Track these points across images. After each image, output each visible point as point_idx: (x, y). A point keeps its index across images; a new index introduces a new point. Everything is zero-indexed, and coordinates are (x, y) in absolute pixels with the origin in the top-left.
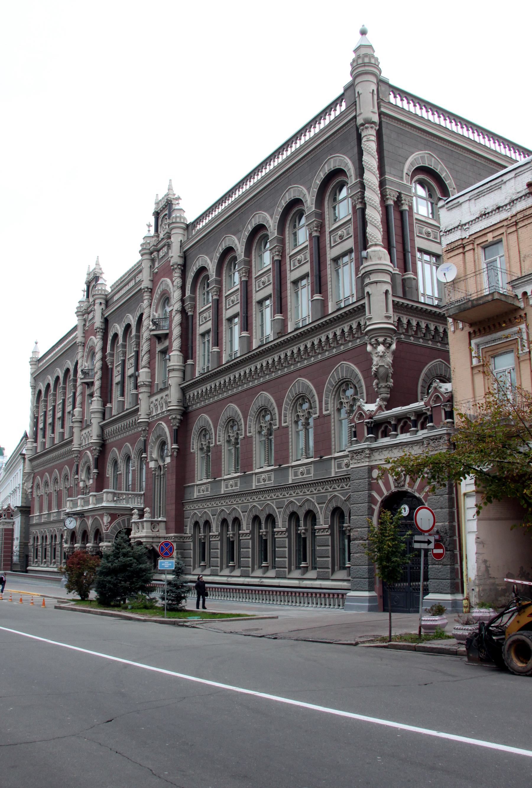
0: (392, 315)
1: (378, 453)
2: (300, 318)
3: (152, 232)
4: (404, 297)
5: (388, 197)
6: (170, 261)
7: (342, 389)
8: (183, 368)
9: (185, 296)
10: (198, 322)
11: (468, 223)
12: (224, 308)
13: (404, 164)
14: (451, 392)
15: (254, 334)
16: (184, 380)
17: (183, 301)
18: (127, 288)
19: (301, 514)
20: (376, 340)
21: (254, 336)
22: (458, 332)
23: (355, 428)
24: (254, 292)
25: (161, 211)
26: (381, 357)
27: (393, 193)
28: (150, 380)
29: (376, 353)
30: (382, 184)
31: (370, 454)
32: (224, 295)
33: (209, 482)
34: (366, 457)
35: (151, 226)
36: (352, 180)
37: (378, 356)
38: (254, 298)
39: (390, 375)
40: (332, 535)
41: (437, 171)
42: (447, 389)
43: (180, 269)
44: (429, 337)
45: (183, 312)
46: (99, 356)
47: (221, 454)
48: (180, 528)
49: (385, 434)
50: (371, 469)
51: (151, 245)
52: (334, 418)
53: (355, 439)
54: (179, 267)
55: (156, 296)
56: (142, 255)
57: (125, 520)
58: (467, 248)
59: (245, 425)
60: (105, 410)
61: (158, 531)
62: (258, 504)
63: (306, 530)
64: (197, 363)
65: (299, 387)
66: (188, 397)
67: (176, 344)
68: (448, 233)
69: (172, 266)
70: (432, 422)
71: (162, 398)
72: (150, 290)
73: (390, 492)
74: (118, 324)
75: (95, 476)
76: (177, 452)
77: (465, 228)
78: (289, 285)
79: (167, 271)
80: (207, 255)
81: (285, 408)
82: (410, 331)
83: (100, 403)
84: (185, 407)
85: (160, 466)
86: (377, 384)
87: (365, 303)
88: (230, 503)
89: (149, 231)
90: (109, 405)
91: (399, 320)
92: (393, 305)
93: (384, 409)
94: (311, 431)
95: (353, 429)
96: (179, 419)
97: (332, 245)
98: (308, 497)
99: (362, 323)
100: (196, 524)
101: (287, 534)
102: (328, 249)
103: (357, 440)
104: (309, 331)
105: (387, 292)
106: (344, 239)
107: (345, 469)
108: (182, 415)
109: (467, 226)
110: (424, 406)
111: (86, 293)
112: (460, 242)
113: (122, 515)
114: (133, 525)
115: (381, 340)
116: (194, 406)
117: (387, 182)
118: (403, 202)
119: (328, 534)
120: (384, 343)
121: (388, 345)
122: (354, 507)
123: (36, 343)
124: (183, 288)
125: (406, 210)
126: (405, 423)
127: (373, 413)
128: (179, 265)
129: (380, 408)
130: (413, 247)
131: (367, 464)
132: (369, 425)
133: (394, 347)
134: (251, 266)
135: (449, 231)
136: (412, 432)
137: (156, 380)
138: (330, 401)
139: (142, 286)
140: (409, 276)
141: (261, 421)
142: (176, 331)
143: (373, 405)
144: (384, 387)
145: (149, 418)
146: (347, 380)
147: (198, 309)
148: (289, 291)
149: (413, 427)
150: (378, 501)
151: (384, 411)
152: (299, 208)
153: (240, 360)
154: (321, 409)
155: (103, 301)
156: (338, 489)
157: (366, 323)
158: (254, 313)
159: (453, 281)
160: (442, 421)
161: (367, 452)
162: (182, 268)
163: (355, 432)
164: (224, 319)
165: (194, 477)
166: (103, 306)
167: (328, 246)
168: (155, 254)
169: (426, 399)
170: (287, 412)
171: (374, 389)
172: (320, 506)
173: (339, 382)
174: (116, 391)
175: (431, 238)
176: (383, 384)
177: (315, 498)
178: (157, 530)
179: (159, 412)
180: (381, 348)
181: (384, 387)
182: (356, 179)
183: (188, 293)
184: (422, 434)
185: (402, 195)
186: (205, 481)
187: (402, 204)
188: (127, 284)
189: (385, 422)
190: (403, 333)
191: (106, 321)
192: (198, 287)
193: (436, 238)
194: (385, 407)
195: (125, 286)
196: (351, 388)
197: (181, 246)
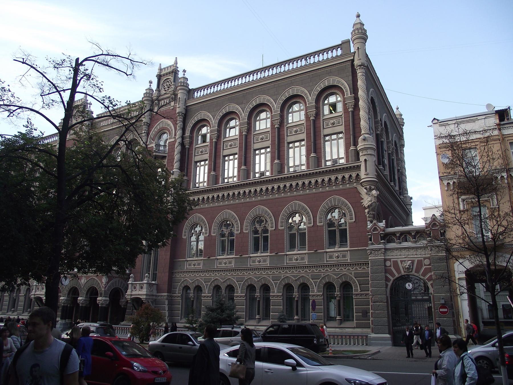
1: (390, 251)
7: (331, 212)
20: (370, 187)
29: (369, 194)
34: (382, 253)
36: (348, 93)
40: (323, 299)
48: (170, 289)
50: (385, 260)
61: (152, 291)
73: (400, 275)
86: (368, 212)
87: (361, 165)
95: (370, 237)
114: (130, 286)
142: (177, 157)
146: (338, 206)
150: (391, 280)
167: (322, 127)
176: (371, 212)
189: (394, 234)
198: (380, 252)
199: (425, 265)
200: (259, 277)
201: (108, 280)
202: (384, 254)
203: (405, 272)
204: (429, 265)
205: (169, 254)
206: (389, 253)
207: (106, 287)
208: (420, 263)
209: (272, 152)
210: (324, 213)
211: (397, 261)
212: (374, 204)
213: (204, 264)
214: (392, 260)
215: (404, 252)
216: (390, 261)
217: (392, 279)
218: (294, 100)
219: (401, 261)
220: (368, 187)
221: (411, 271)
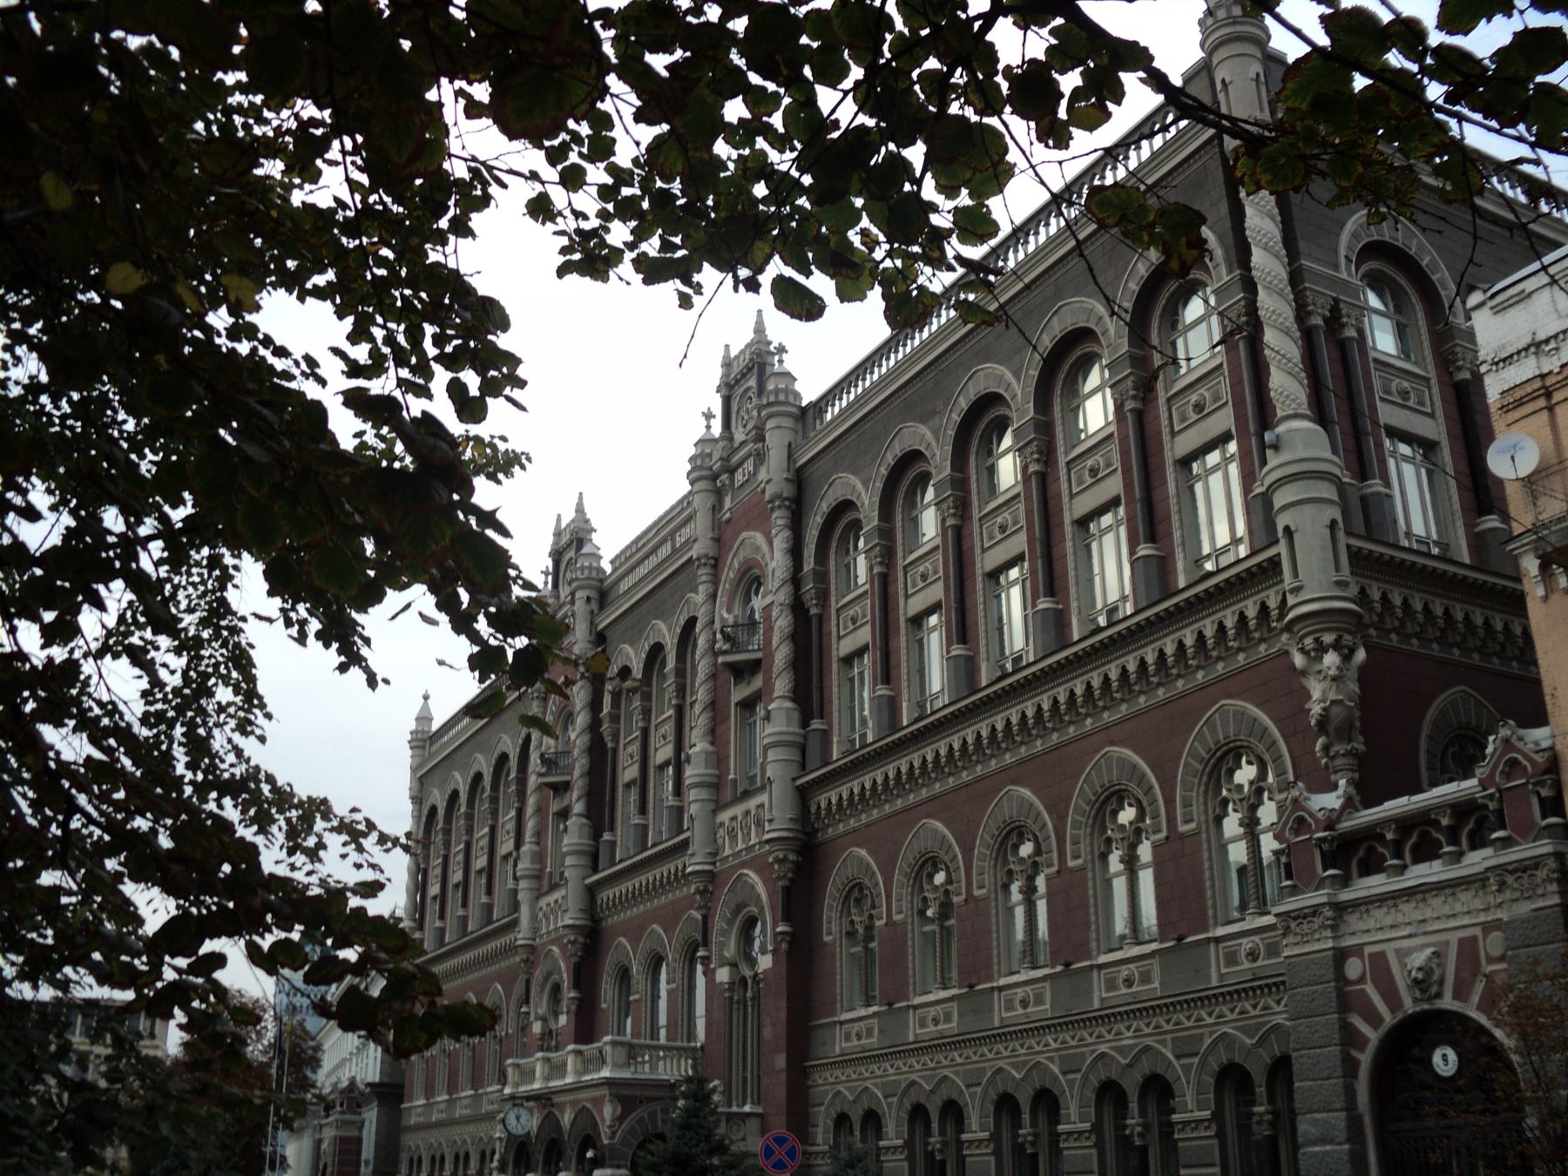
0: (1349, 580)
1: (1357, 915)
2: (1099, 605)
3: (717, 429)
4: (1368, 537)
5: (1310, 308)
6: (763, 491)
8: (801, 740)
9: (801, 570)
10: (834, 629)
11: (1555, 336)
12: (901, 593)
13: (1338, 235)
14: (1552, 748)
15: (983, 649)
16: (804, 769)
17: (795, 580)
18: (653, 561)
19: (1131, 1086)
20: (1316, 640)
21: (983, 655)
22: (1556, 598)
23: (1288, 855)
24: (978, 551)
25: (737, 382)
26: (1334, 679)
27: (1321, 301)
28: (717, 772)
29: (1319, 672)
30: (1296, 278)
31: (1334, 919)
32: (901, 563)
33: (875, 1014)
34: (1323, 927)
35: (714, 417)
37: (1325, 678)
38: (978, 565)
39: (1358, 724)
40: (1221, 1135)
41: (1412, 253)
42: (1537, 744)
43: (787, 508)
44: (1432, 633)
45: (797, 607)
46: (581, 720)
47: (906, 942)
49: (1370, 867)
50: (1341, 956)
51: (715, 458)
52: (1209, 841)
53: (1289, 883)
54: (787, 503)
55: (729, 574)
56: (692, 484)
57: (655, 1112)
58: (1557, 397)
59: (968, 869)
60: (598, 850)
62: (1012, 1064)
63: (1146, 1126)
64: (836, 727)
65: (1109, 770)
66: (813, 809)
67: (782, 685)
68: (1501, 365)
69: (769, 502)
70: (1503, 827)
71: (747, 813)
72: (712, 562)
73: (1400, 1016)
74: (631, 645)
75: (574, 1007)
76: (790, 943)
77: (1547, 349)
78: (1068, 529)
79: (756, 516)
80: (854, 473)
81: (1074, 821)
82: (1388, 619)
83: (586, 830)
84: (806, 834)
85: (743, 980)
86: (1326, 748)
87: (1279, 554)
88: (931, 1065)
89: (708, 427)
90: (606, 836)
91: (1363, 591)
92: (1349, 557)
93: (1359, 806)
94: (1146, 879)
96: (793, 862)
97: (1177, 429)
98: (1149, 1041)
99: (1273, 603)
100: (842, 1120)
101: (1093, 1138)
102: (1166, 437)
103: (1294, 887)
104: (1142, 627)
105: (1333, 524)
106: (1206, 412)
107: (1247, 965)
108: (799, 853)
109: (1552, 345)
110: (1480, 788)
111: (550, 578)
112: (1537, 384)
113: (650, 1100)
115: (1328, 638)
116: (830, 830)
117: (1306, 275)
118: (1344, 320)
119: (1208, 1134)
120: (1336, 646)
121: (1346, 651)
122: (1301, 1056)
123: (426, 698)
124: (796, 552)
125: (1351, 339)
126: (1424, 836)
127: (1336, 814)
128: (786, 499)
129: (1349, 804)
130: (1376, 423)
131: (1330, 944)
132: (1326, 847)
133: (1361, 655)
134: (968, 492)
135: (1504, 360)
136: (1447, 857)
137: (732, 771)
138: (1196, 797)
139: (694, 553)
140: (1374, 489)
141: (1011, 858)
142: (782, 654)
143: (1333, 795)
144: (1343, 755)
145: (714, 864)
146: (1238, 743)
147: (833, 599)
148: (1069, 544)
149: (1448, 845)
150: (1366, 1040)
151: (1357, 810)
152: (1086, 350)
153: (952, 713)
154: (1171, 820)
155: (593, 594)
156: (1230, 1017)
157: (1284, 601)
158: (980, 600)
159: (1529, 477)
160: (1533, 823)
161: (1328, 913)
162: (794, 507)
163: (1288, 866)
164: (902, 619)
165: (834, 1002)
166: (594, 606)
167: (1166, 432)
168: (724, 477)
169: (1481, 770)
170: (1082, 832)
171: (1316, 761)
172: (1184, 1061)
173: (1218, 750)
174: (626, 804)
175: (1411, 403)
176: (1339, 748)
177: (1169, 1043)
178: (740, 1136)
179: (740, 846)
180: (1331, 659)
181: (1343, 755)
182: (1230, 271)
183: (809, 564)
184: (1478, 860)
185: (1342, 306)
186: (863, 1012)
187: (1343, 326)
188: (654, 551)
189: (1371, 833)
190: (1373, 625)
191: (600, 638)
192: (833, 550)
193: (1422, 403)
194: (1361, 802)
195: (647, 556)
196: (1249, 763)
197: (789, 457)
198: (1318, 921)
199: (1491, 960)
200: (1024, 1063)
201: (619, 1111)
202: (1334, 928)
203: (1415, 1000)
204: (1502, 958)
205: (783, 1004)
206: (1354, 921)
207: (614, 1134)
208: (1468, 948)
209: (1033, 572)
210: (1196, 781)
211: (1382, 954)
212: (1336, 710)
213: (881, 1030)
214: (1368, 950)
215: (1409, 912)
216: (1361, 956)
217: (1373, 1036)
218: (1078, 353)
219: (1398, 951)
220: (1309, 641)
221: (1439, 995)
